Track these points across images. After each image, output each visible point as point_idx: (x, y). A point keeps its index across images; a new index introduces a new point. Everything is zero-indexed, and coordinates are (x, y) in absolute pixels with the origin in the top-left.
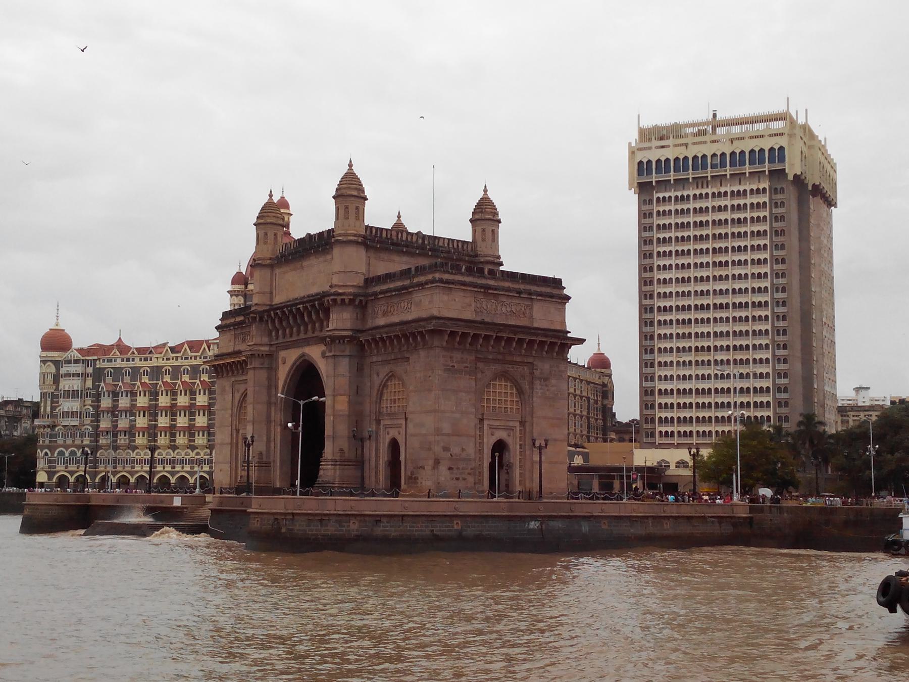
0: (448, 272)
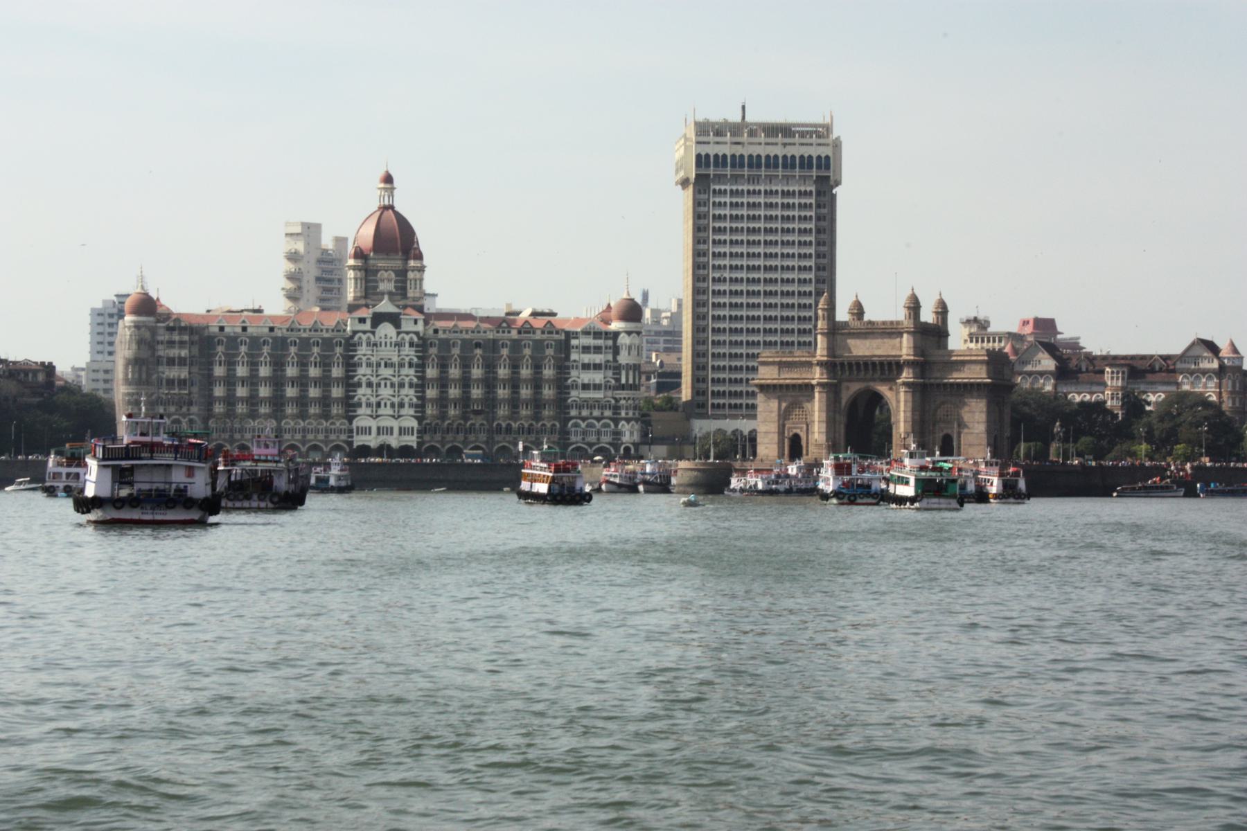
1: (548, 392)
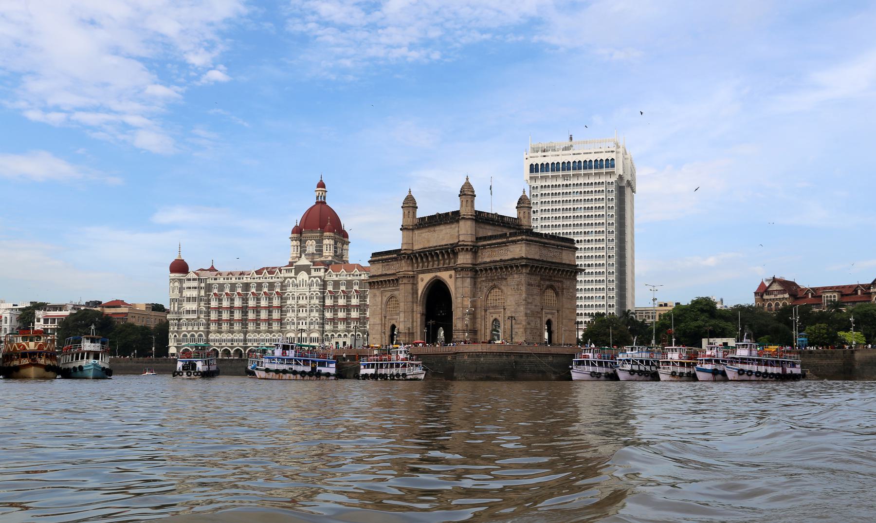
0: (528, 236)
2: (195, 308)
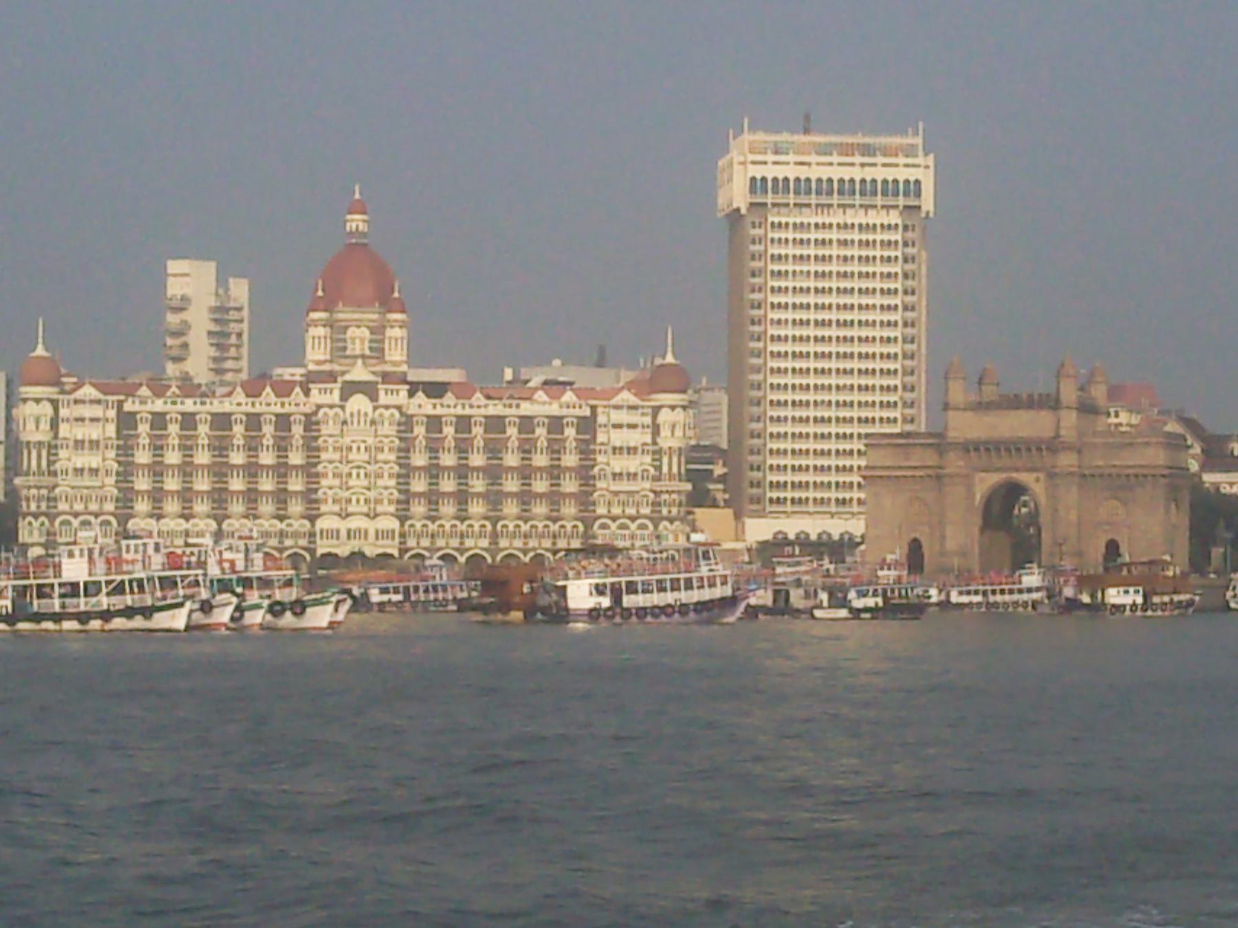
1: (570, 485)
2: (98, 464)
